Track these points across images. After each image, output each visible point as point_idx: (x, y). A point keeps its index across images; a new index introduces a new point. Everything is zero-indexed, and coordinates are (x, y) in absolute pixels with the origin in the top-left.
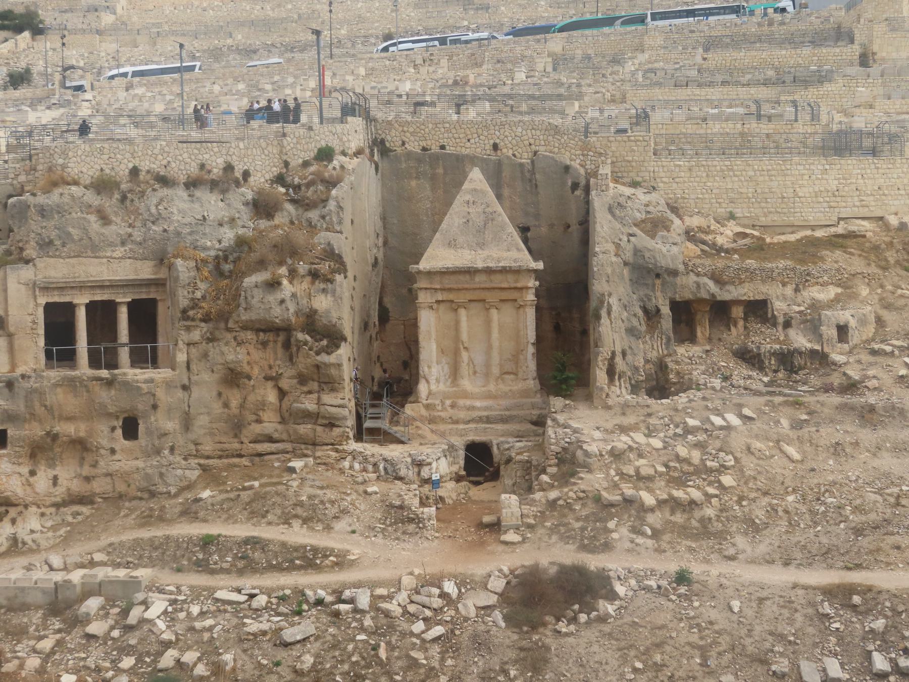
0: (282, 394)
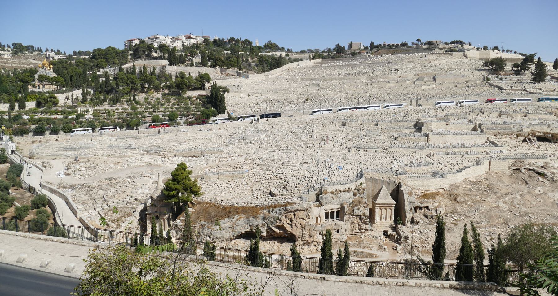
0: (359, 225)
